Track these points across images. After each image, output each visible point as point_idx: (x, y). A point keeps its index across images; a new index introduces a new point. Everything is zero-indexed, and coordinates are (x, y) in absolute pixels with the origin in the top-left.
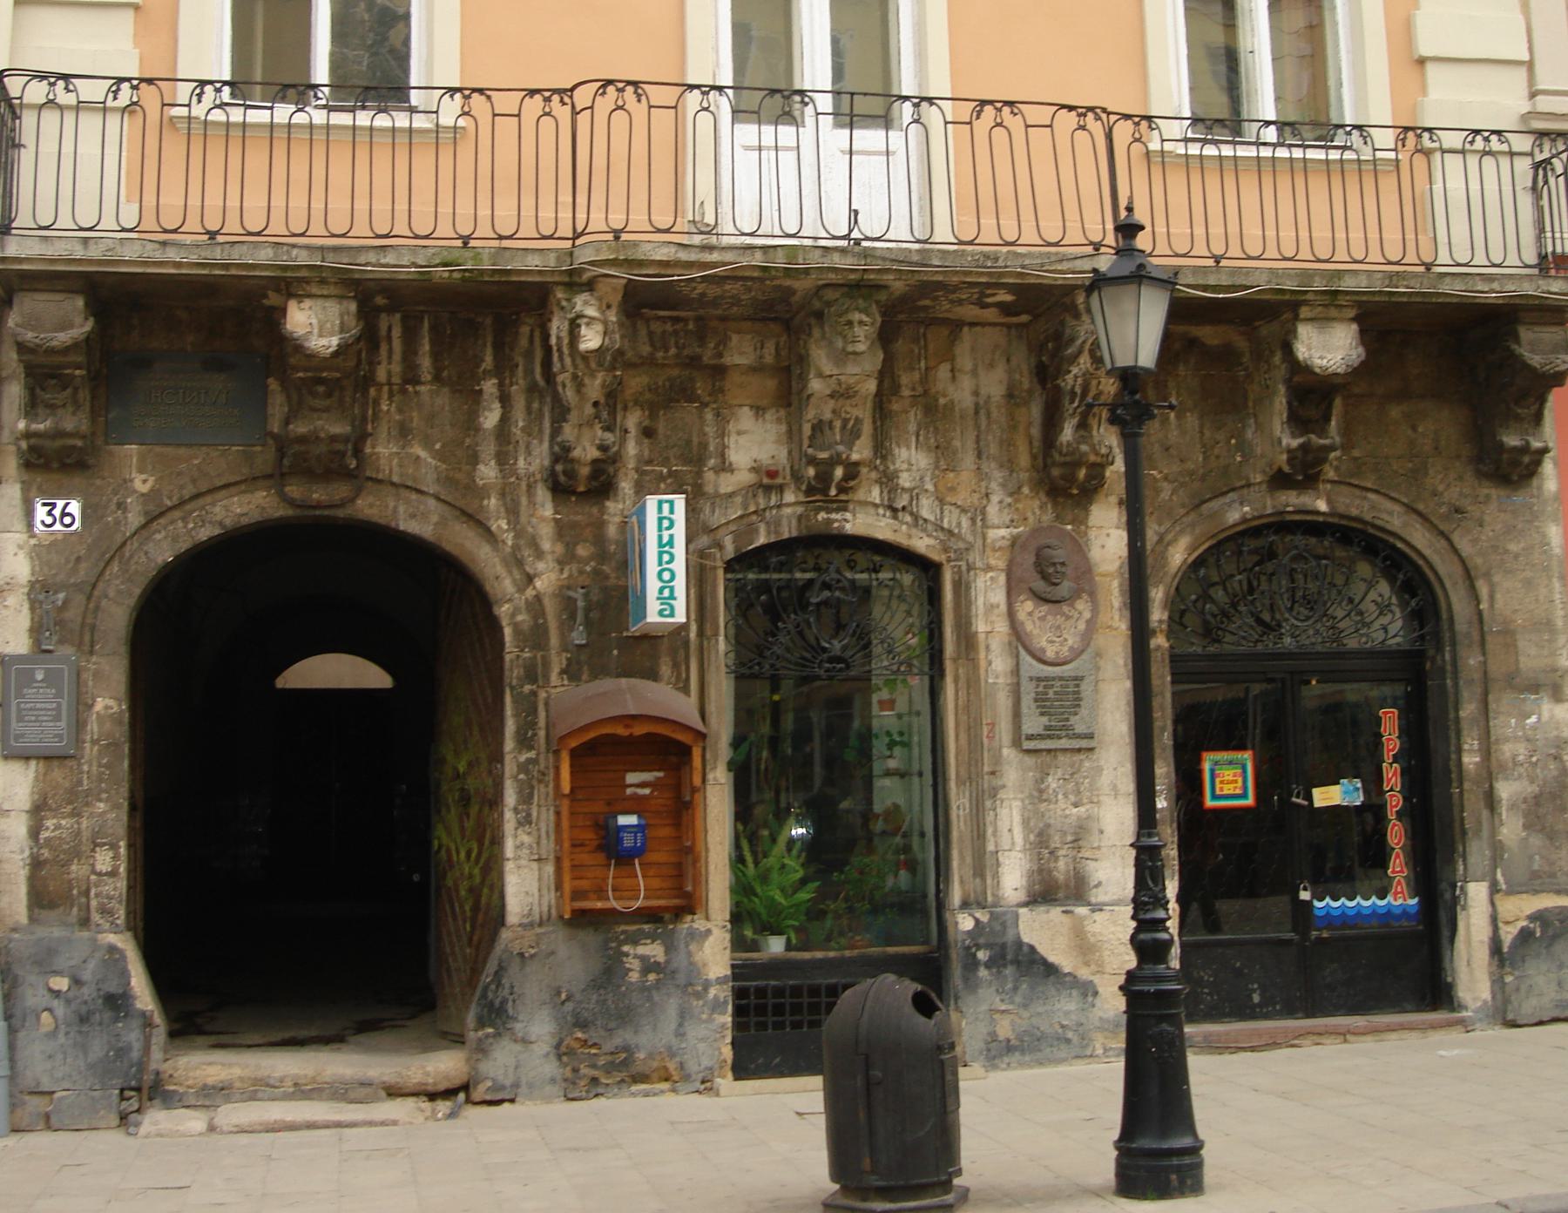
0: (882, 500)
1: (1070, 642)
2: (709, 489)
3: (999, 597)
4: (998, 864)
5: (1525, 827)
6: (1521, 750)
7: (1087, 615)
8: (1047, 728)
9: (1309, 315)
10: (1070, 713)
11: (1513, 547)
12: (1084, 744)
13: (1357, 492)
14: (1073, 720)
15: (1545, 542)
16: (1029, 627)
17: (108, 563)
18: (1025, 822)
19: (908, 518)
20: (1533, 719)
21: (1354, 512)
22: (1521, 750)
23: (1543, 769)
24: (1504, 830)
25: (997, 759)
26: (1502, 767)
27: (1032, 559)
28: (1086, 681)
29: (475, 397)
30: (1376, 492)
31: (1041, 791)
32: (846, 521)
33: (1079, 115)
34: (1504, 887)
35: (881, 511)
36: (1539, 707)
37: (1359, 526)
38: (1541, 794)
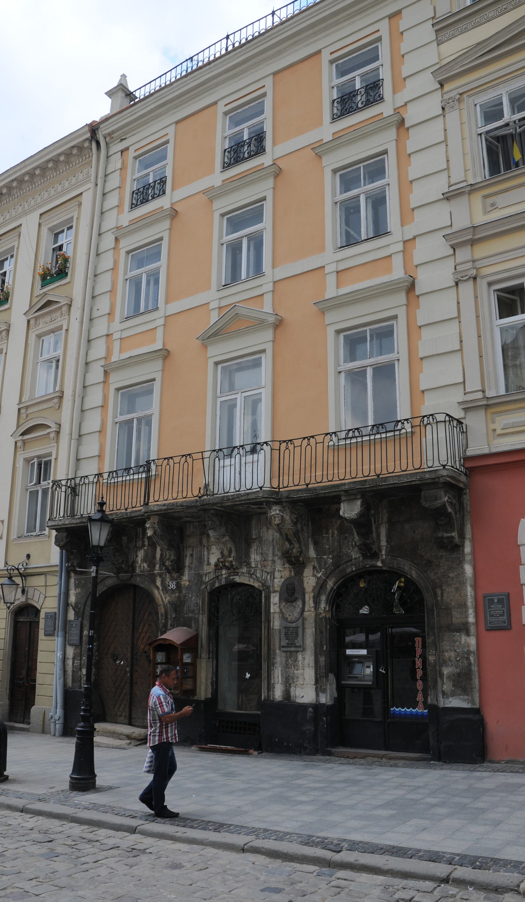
5: (453, 686)
6: (452, 654)
7: (301, 606)
8: (288, 644)
9: (345, 499)
11: (451, 575)
14: (296, 641)
15: (463, 573)
16: (283, 611)
18: (282, 674)
20: (458, 643)
23: (462, 663)
25: (275, 654)
28: (300, 628)
30: (400, 557)
36: (461, 638)
38: (460, 673)
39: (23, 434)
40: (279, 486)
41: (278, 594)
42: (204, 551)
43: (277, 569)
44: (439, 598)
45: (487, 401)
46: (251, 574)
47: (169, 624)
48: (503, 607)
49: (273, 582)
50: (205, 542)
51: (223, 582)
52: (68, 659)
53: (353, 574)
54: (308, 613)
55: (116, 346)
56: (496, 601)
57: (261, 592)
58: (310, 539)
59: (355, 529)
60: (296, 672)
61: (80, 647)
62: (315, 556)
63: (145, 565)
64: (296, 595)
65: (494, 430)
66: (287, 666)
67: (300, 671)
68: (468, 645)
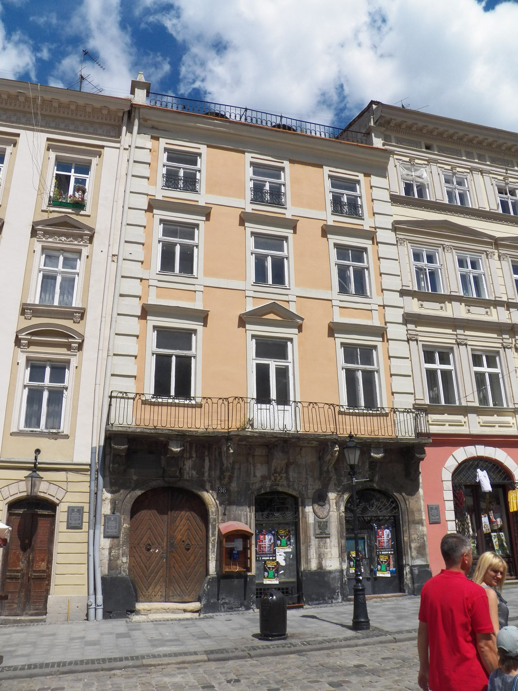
4: (311, 562)
5: (417, 553)
6: (416, 536)
7: (329, 508)
12: (328, 536)
14: (326, 531)
16: (317, 511)
18: (316, 553)
22: (416, 536)
24: (413, 554)
25: (310, 539)
39: (32, 334)
41: (311, 500)
42: (250, 467)
43: (309, 484)
46: (289, 486)
49: (307, 492)
50: (251, 459)
51: (268, 490)
54: (332, 513)
55: (153, 291)
60: (325, 550)
63: (194, 473)
66: (319, 547)
67: (329, 550)
68: (423, 531)
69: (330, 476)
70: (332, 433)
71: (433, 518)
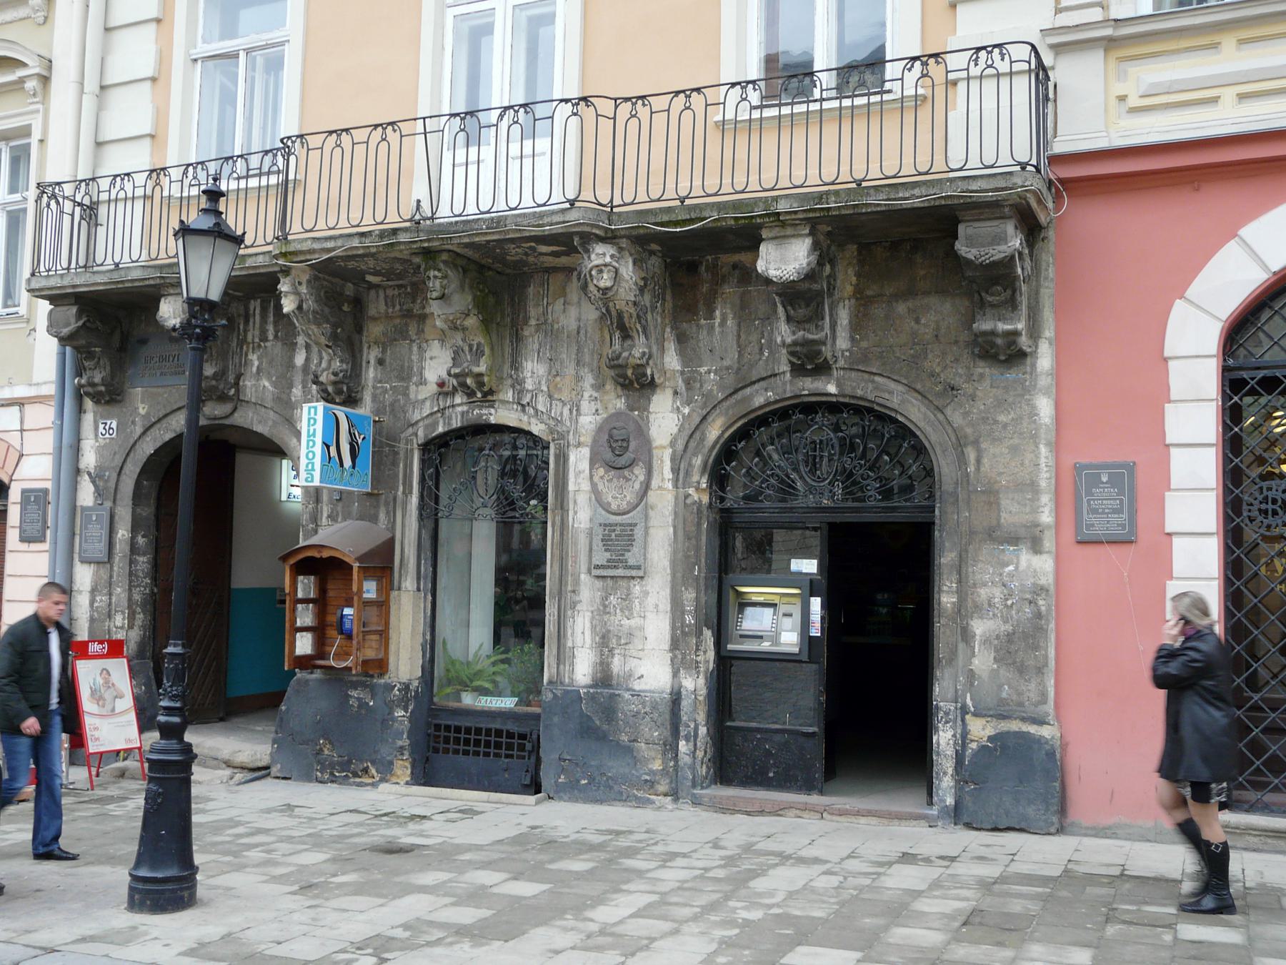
0: (514, 398)
1: (628, 498)
2: (412, 396)
3: (585, 465)
6: (998, 593)
7: (642, 478)
8: (609, 561)
10: (625, 550)
11: (1002, 418)
12: (634, 573)
13: (866, 376)
14: (628, 555)
15: (1033, 413)
16: (600, 487)
17: (128, 455)
18: (593, 628)
19: (532, 411)
20: (1011, 568)
21: (859, 393)
24: (976, 661)
25: (577, 582)
26: (977, 608)
27: (606, 437)
28: (638, 527)
29: (292, 346)
31: (605, 606)
32: (491, 414)
33: (573, 105)
34: (972, 709)
35: (515, 406)
37: (867, 404)
40: (611, 201)
44: (971, 469)
45: (1115, 28)
46: (523, 406)
47: (325, 515)
48: (1121, 493)
50: (412, 331)
51: (456, 423)
52: (80, 592)
53: (767, 409)
56: (1104, 479)
57: (546, 447)
58: (668, 330)
59: (784, 307)
60: (625, 622)
61: (108, 566)
62: (679, 368)
64: (629, 456)
65: (1122, 99)
66: (604, 609)
69: (631, 361)
70: (567, 205)
71: (1093, 519)
